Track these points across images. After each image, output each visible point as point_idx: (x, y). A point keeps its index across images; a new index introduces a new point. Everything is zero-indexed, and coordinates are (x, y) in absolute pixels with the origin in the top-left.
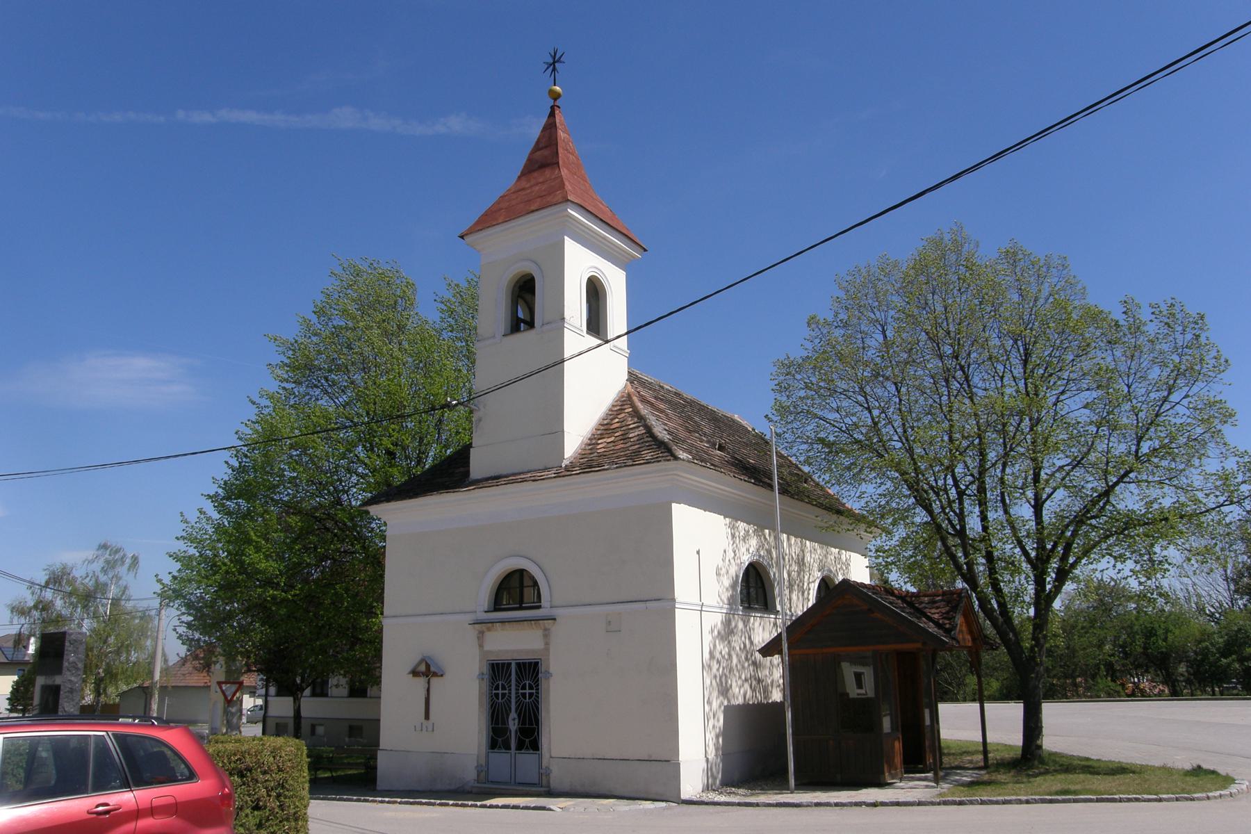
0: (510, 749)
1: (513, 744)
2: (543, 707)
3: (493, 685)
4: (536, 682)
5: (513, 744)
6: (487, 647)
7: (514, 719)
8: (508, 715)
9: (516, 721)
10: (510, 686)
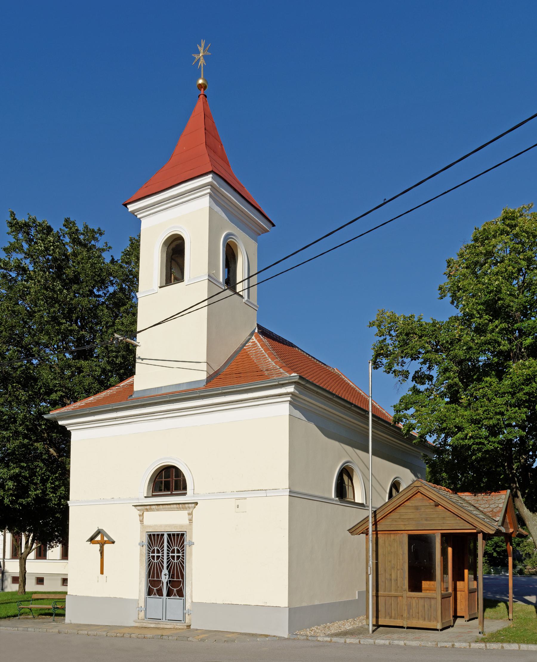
0: (162, 596)
1: (165, 592)
2: (187, 566)
3: (150, 549)
4: (149, 560)
5: (165, 592)
6: (146, 522)
7: (165, 575)
8: (161, 572)
9: (167, 576)
10: (163, 550)
